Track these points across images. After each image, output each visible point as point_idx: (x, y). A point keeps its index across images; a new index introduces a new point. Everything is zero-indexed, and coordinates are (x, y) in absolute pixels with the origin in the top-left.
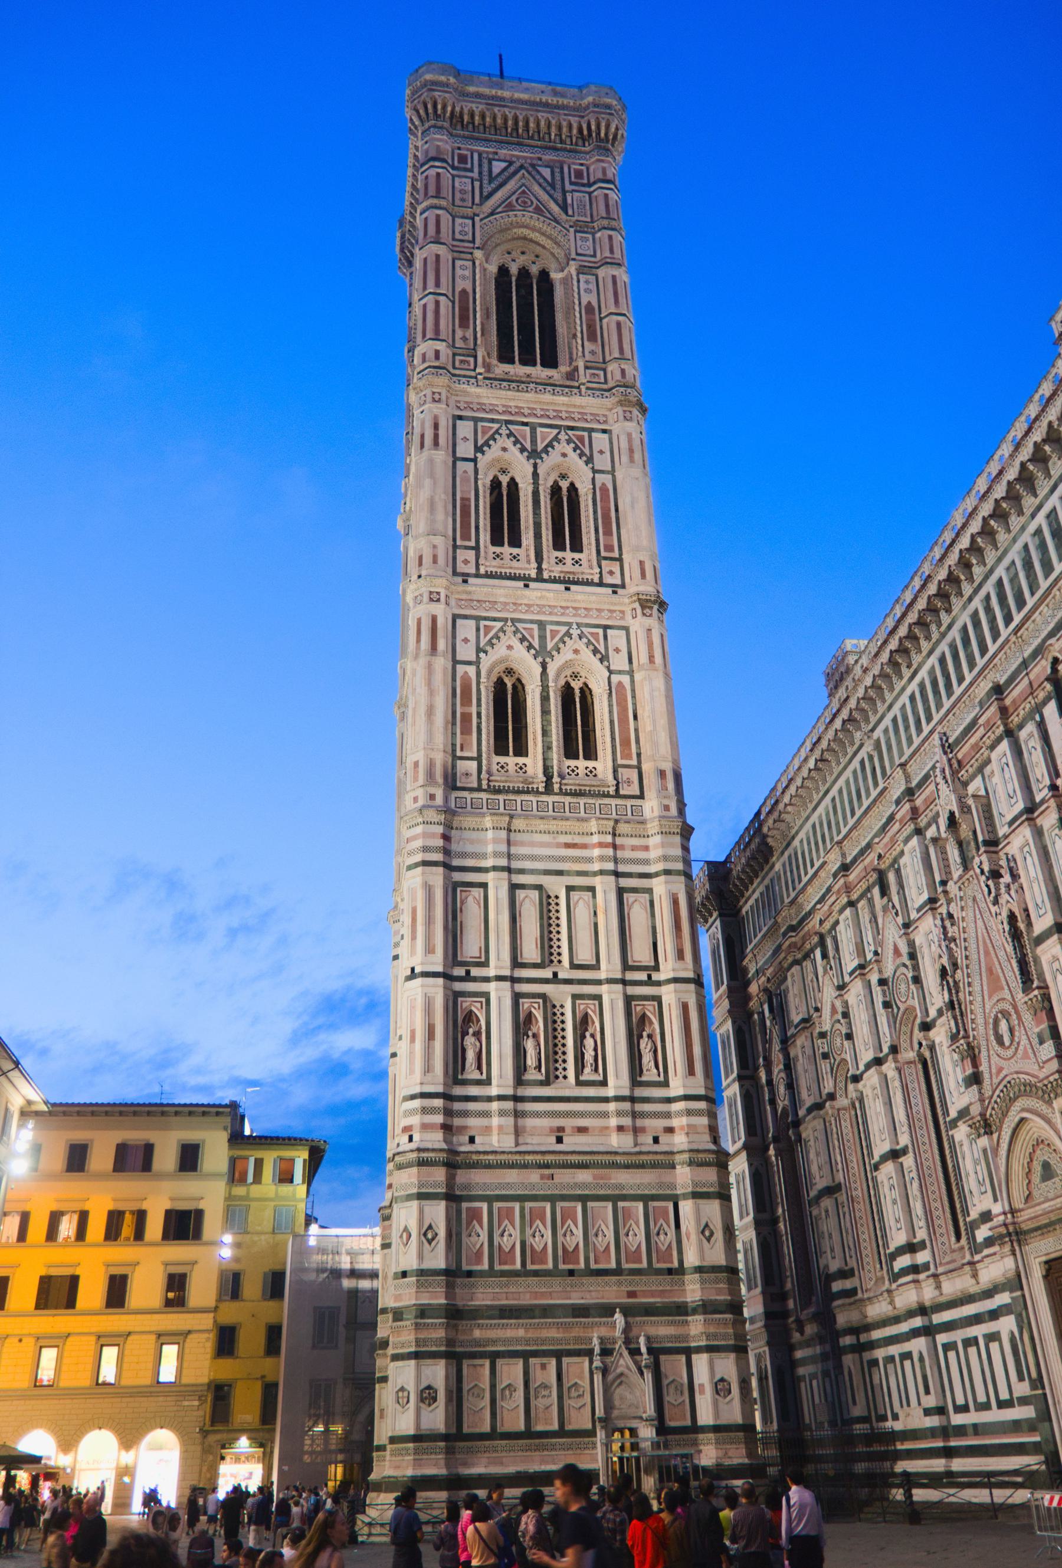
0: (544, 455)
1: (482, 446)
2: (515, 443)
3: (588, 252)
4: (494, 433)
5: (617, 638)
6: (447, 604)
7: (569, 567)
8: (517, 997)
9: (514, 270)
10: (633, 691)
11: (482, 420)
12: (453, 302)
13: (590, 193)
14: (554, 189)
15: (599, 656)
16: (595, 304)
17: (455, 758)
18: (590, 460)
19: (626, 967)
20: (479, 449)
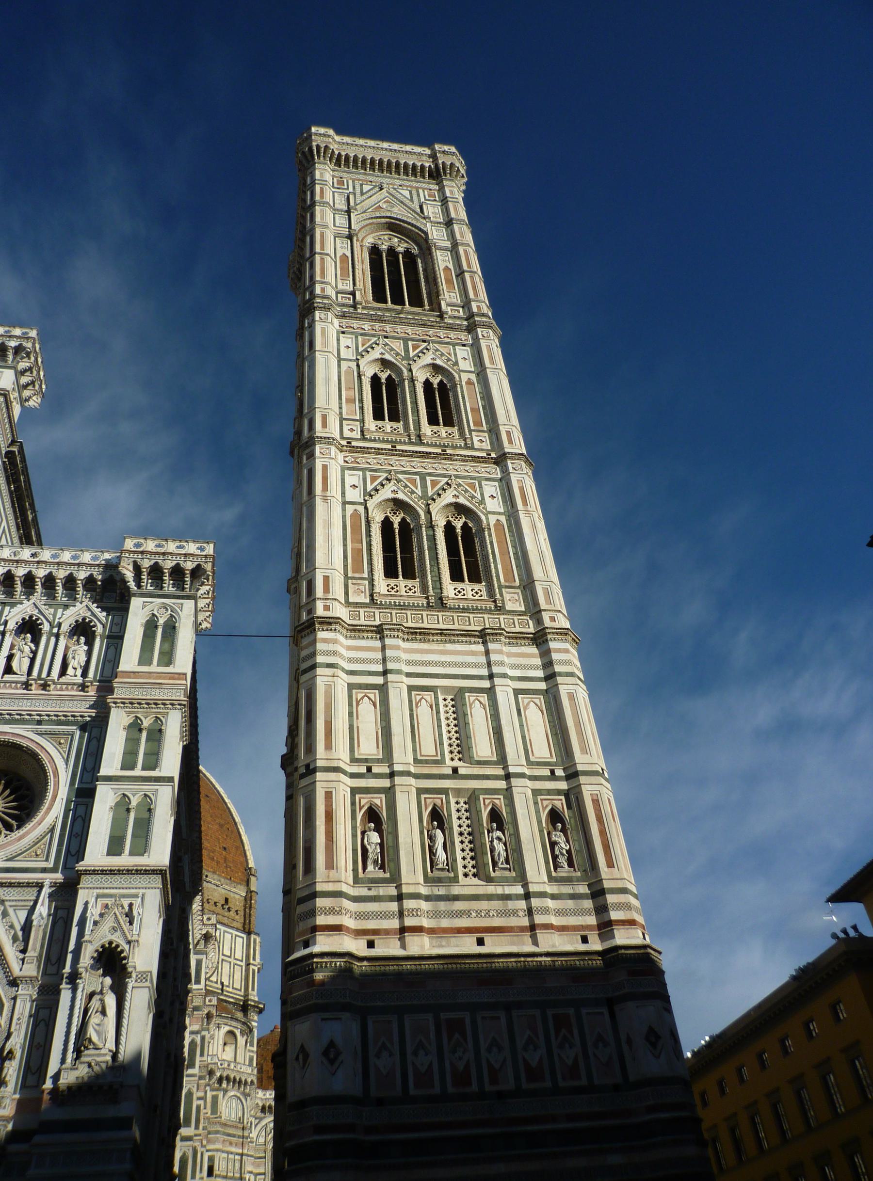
1: (362, 352)
3: (443, 238)
8: (420, 791)
9: (384, 247)
10: (510, 527)
12: (335, 263)
19: (530, 763)
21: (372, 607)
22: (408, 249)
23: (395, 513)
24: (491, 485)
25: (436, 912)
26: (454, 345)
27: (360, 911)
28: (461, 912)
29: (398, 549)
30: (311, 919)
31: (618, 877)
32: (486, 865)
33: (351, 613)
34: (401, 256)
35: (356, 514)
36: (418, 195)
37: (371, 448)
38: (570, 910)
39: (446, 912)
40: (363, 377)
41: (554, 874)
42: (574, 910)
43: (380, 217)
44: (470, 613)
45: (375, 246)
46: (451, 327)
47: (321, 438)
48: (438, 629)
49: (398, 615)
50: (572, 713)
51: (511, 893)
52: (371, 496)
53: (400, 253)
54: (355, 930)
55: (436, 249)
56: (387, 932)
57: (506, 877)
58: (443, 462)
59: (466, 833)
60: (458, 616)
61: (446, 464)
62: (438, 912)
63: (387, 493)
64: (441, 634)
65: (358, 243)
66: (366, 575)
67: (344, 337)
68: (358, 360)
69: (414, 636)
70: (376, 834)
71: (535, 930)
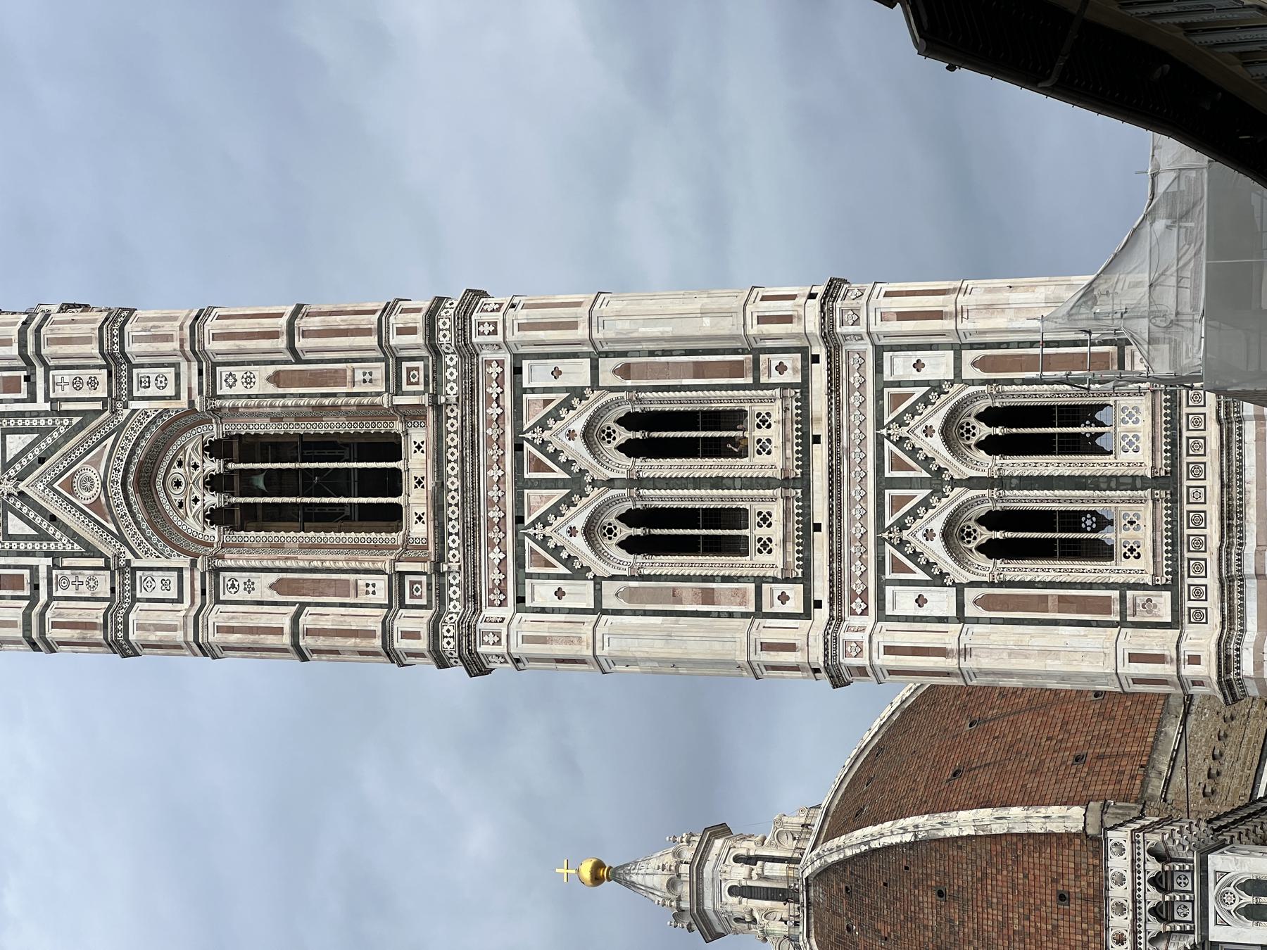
0: (575, 469)
2: (558, 514)
3: (171, 378)
4: (546, 549)
5: (900, 366)
6: (863, 630)
7: (774, 433)
11: (520, 564)
12: (303, 605)
13: (47, 369)
14: (47, 431)
15: (933, 396)
16: (271, 369)
17: (1122, 623)
18: (578, 393)
20: (580, 573)
21: (1181, 588)
22: (204, 449)
23: (969, 535)
24: (892, 365)
26: (519, 391)
29: (1049, 535)
33: (1192, 620)
34: (231, 466)
35: (984, 602)
36: (22, 414)
37: (831, 569)
40: (646, 572)
43: (129, 505)
44: (1180, 436)
45: (208, 516)
46: (470, 392)
47: (826, 656)
48: (1222, 491)
49: (1192, 549)
52: (943, 575)
53: (225, 468)
55: (221, 397)
58: (844, 443)
60: (1188, 455)
61: (849, 439)
63: (936, 550)
64: (1229, 487)
65: (226, 556)
66: (1115, 594)
67: (533, 599)
68: (595, 576)
69: (1234, 529)
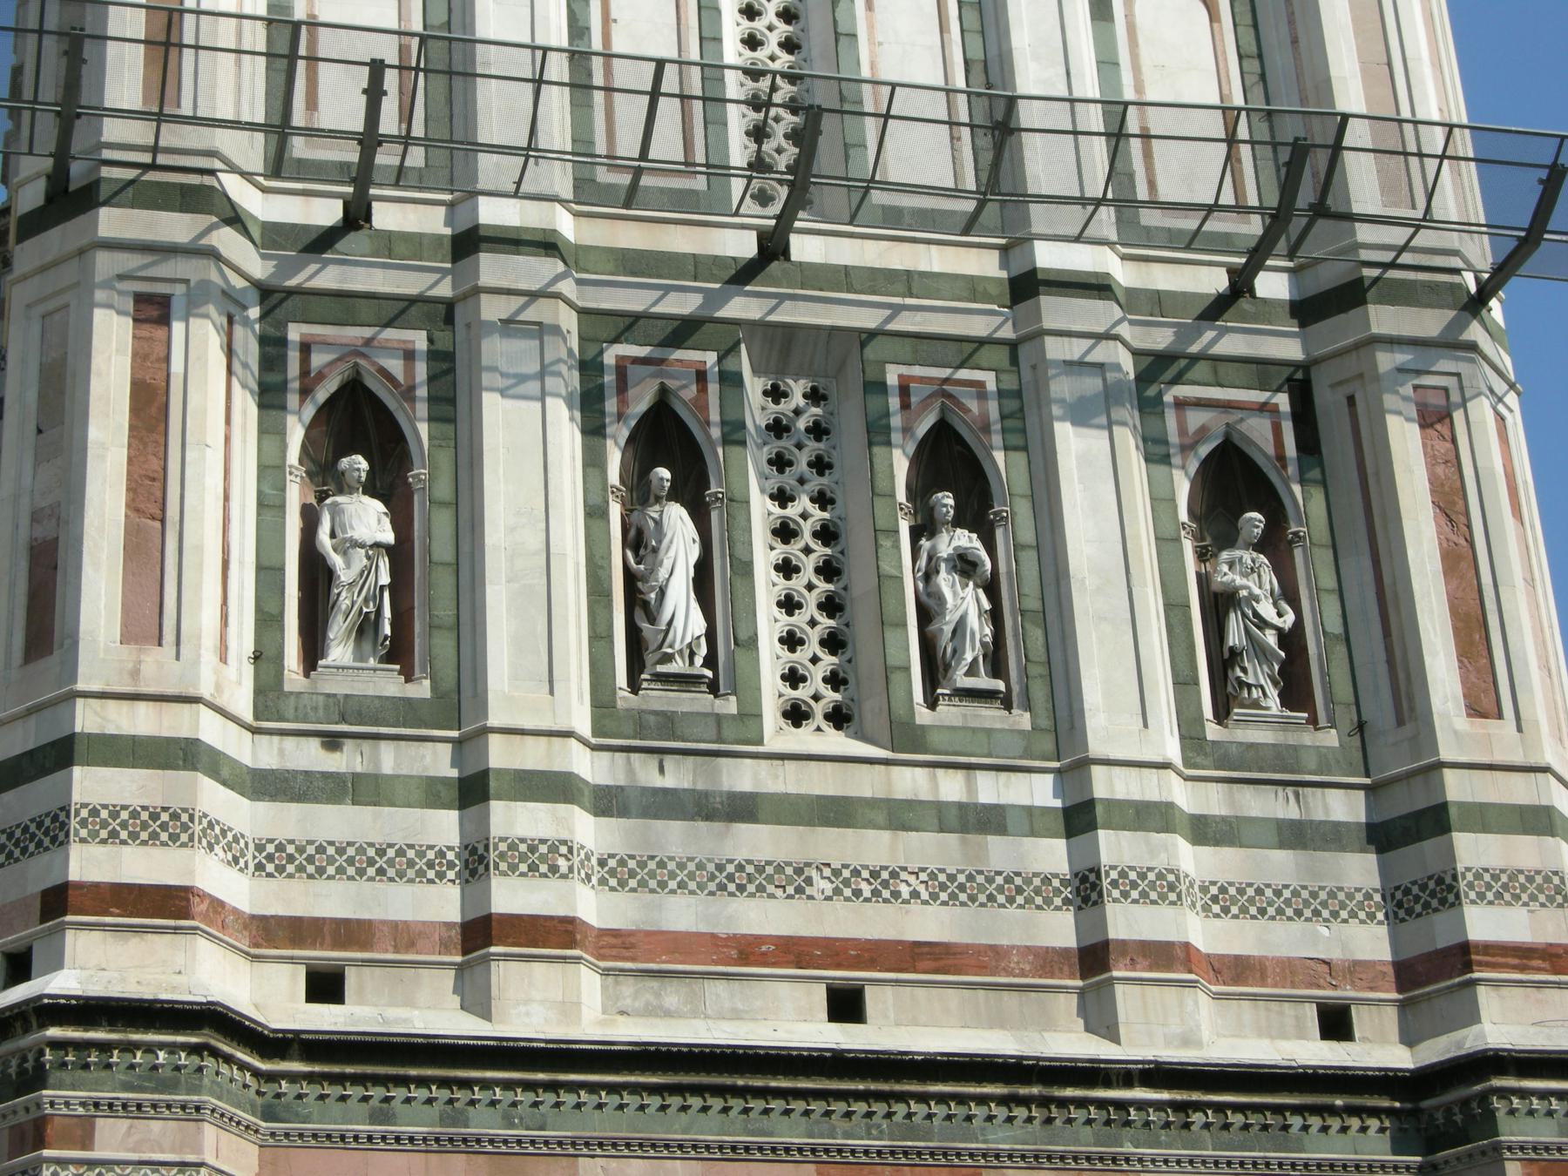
25: (642, 865)
27: (281, 836)
28: (760, 869)
30: (45, 857)
31: (1517, 758)
32: (892, 672)
38: (1278, 893)
39: (691, 866)
41: (1213, 731)
42: (1295, 893)
50: (1355, 20)
51: (1002, 801)
54: (253, 917)
56: (405, 935)
57: (989, 732)
59: (807, 528)
62: (652, 865)
70: (377, 506)
71: (1107, 968)
